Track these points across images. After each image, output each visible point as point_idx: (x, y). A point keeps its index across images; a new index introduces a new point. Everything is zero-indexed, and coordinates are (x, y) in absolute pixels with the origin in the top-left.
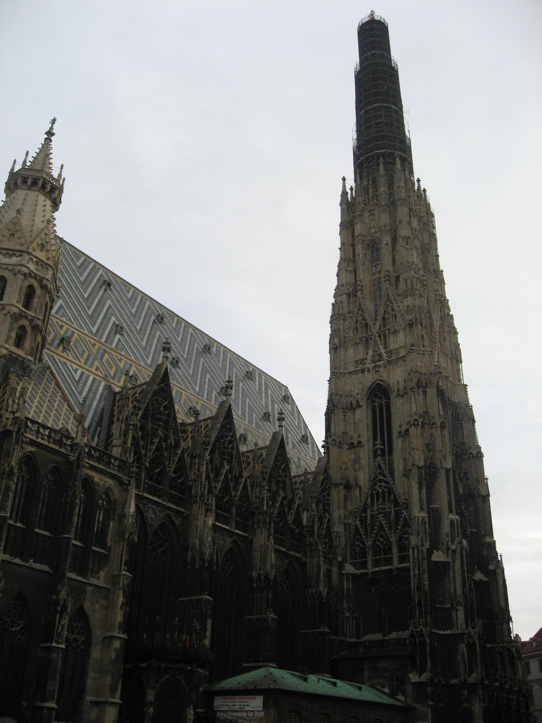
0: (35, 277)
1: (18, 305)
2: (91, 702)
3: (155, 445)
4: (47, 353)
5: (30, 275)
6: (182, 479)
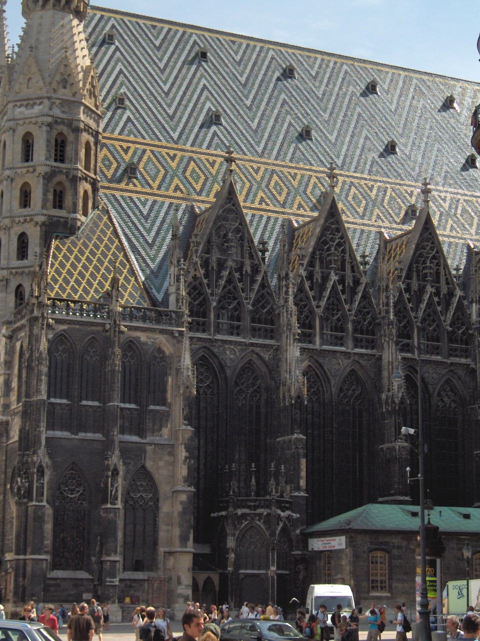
0: (63, 122)
1: (48, 162)
2: (165, 552)
3: (225, 279)
4: (105, 195)
5: (57, 121)
6: (269, 307)
